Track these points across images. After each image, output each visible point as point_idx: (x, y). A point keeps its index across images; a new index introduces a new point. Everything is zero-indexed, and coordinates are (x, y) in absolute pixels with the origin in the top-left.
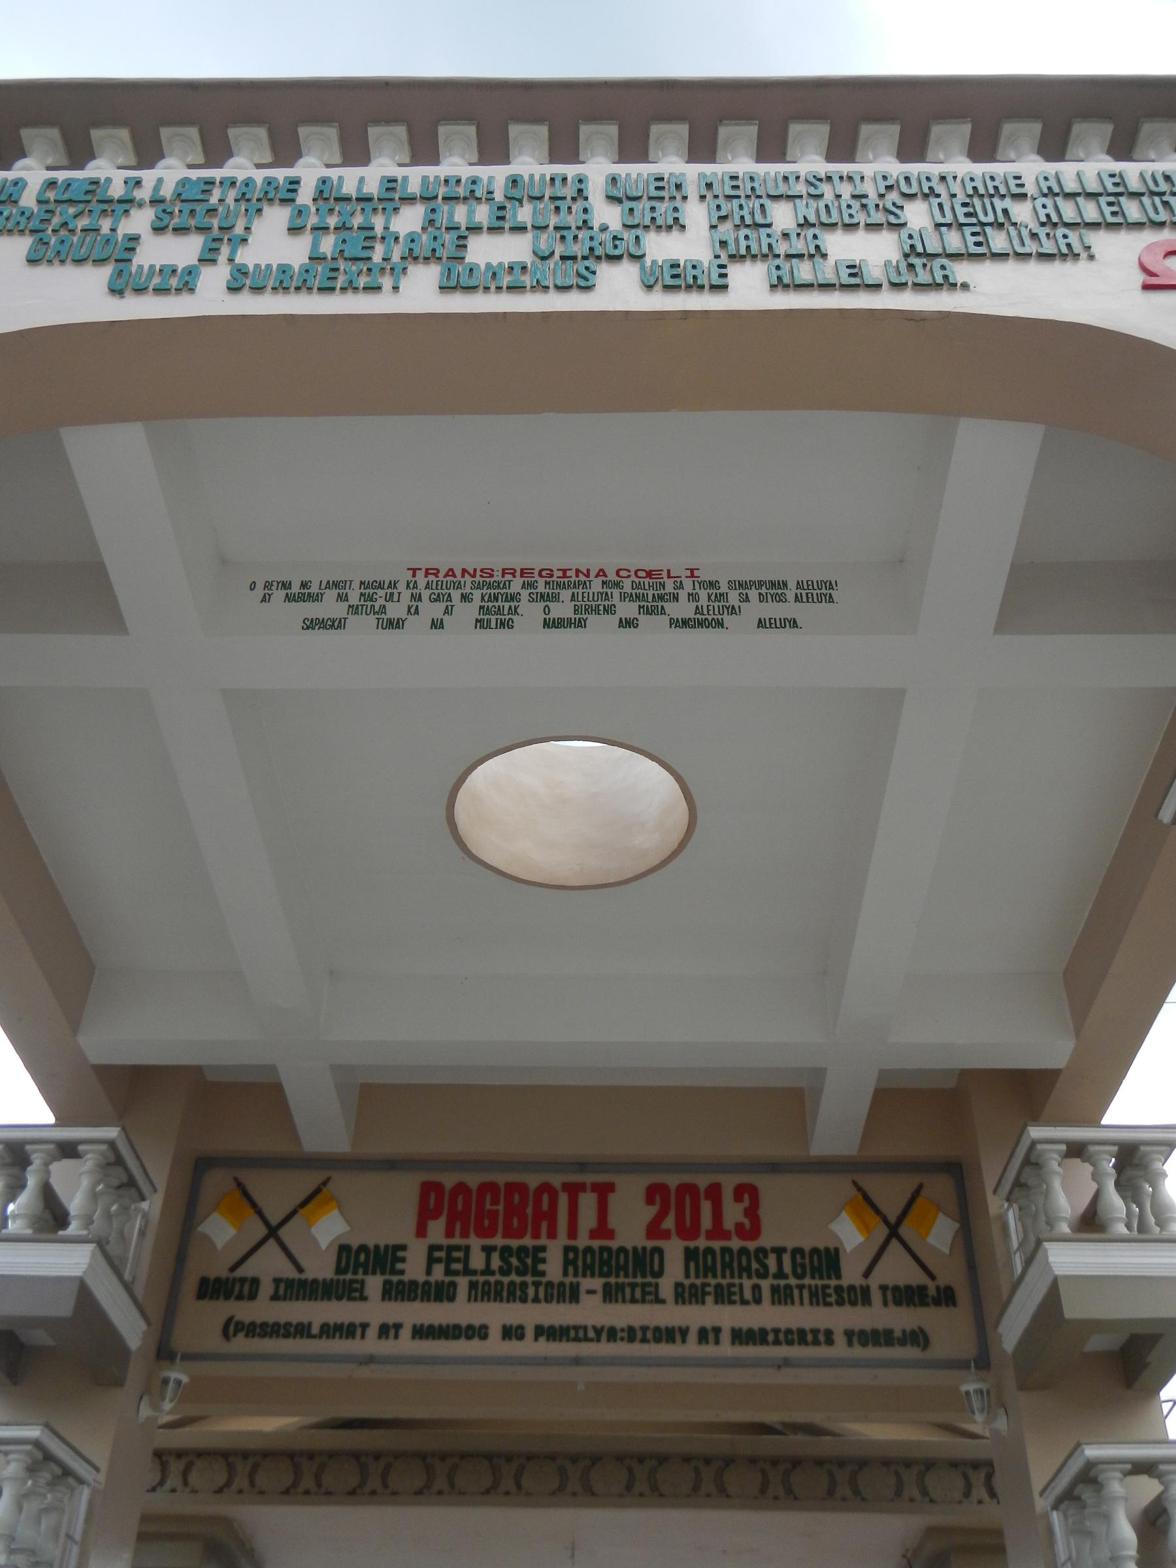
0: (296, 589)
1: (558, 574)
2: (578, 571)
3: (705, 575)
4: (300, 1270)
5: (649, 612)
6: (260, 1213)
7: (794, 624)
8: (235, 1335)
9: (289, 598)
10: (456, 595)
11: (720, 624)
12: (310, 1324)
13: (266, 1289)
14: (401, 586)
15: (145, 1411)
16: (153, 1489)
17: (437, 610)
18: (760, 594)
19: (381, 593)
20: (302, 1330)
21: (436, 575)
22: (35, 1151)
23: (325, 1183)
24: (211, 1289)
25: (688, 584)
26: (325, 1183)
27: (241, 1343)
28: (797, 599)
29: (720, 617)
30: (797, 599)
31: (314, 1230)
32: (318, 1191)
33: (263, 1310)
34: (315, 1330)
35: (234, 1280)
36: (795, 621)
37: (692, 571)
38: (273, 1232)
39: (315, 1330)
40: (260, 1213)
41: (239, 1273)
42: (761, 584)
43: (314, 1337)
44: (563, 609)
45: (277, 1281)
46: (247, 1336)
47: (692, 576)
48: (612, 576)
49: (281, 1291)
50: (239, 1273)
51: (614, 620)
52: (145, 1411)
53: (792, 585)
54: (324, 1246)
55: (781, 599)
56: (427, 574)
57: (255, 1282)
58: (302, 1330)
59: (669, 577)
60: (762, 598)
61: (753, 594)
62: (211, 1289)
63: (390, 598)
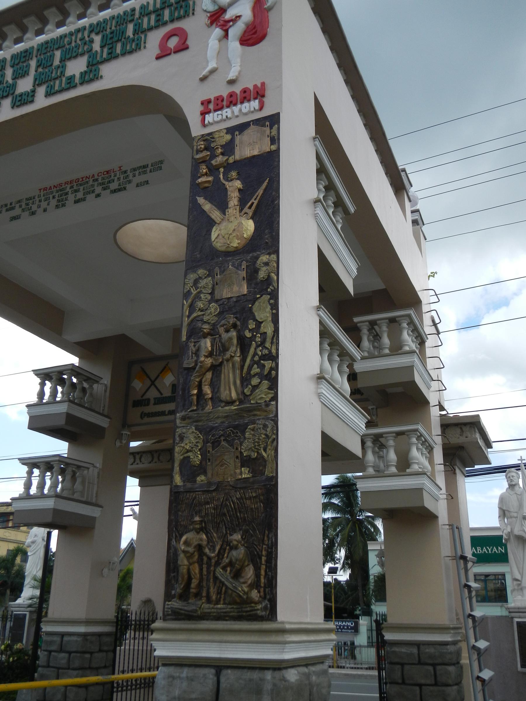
0: (9, 206)
1: (81, 180)
2: (87, 177)
3: (123, 169)
4: (161, 394)
5: (104, 189)
6: (148, 377)
7: (147, 182)
8: (144, 417)
9: (7, 210)
10: (51, 196)
11: (125, 189)
12: (165, 411)
13: (152, 402)
14: (36, 197)
15: (118, 444)
16: (150, 463)
17: (44, 204)
18: (139, 172)
19: (31, 201)
20: (163, 413)
21: (46, 190)
22: (53, 375)
23: (167, 365)
24: (137, 404)
25: (118, 173)
26: (167, 365)
27: (146, 420)
28: (150, 172)
29: (125, 186)
30: (150, 172)
31: (164, 381)
32: (165, 367)
33: (152, 408)
34: (167, 413)
35: (143, 400)
36: (148, 181)
37: (120, 167)
38: (153, 383)
39: (167, 413)
40: (148, 377)
41: (144, 397)
42: (140, 167)
43: (167, 415)
44: (80, 195)
45: (155, 399)
46: (147, 417)
47: (120, 170)
48: (96, 177)
49: (156, 402)
50: (144, 397)
51: (94, 195)
52: (118, 444)
53: (149, 166)
54: (168, 386)
55: (145, 172)
56: (44, 190)
57: (149, 400)
58: (163, 413)
59: (113, 172)
60: (140, 174)
61: (137, 173)
62: (137, 404)
63: (33, 204)
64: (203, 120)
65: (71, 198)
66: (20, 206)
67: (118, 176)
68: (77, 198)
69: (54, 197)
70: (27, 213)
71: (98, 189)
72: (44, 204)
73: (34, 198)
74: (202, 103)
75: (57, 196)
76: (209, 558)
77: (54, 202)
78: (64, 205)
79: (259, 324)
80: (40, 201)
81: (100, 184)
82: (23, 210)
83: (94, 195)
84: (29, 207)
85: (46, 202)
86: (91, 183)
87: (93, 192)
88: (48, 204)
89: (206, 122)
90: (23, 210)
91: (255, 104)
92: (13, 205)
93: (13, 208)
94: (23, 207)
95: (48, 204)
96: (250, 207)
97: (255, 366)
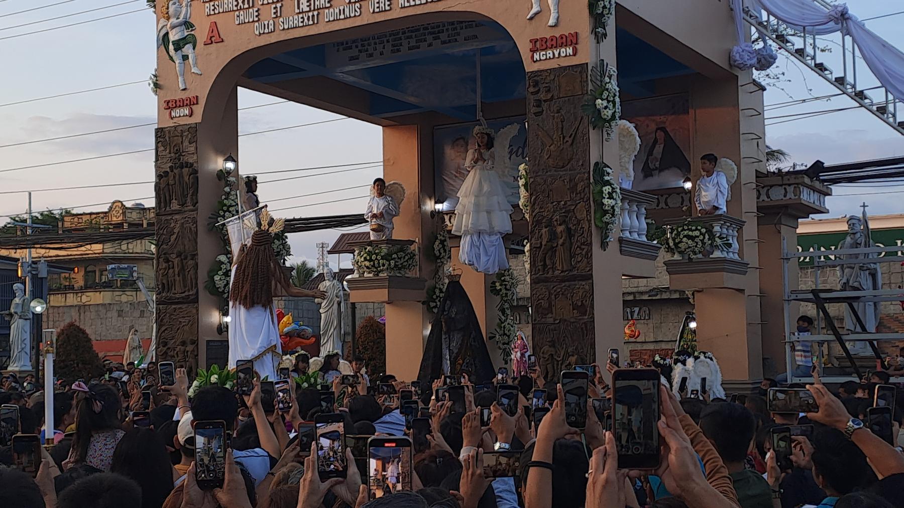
5: (435, 39)
9: (344, 49)
17: (379, 47)
44: (413, 43)
64: (533, 57)
65: (405, 43)
66: (357, 47)
67: (446, 27)
68: (411, 44)
69: (388, 41)
70: (364, 54)
71: (430, 38)
72: (379, 47)
73: (369, 39)
74: (531, 41)
75: (390, 40)
76: (558, 361)
77: (389, 47)
78: (398, 51)
79: (579, 222)
80: (375, 44)
81: (431, 33)
82: (360, 51)
83: (426, 44)
84: (366, 48)
85: (382, 45)
86: (422, 31)
87: (425, 41)
88: (384, 48)
89: (535, 60)
90: (360, 51)
91: (570, 51)
92: (349, 45)
93: (351, 48)
94: (360, 48)
95: (384, 48)
96: (570, 137)
97: (578, 249)
